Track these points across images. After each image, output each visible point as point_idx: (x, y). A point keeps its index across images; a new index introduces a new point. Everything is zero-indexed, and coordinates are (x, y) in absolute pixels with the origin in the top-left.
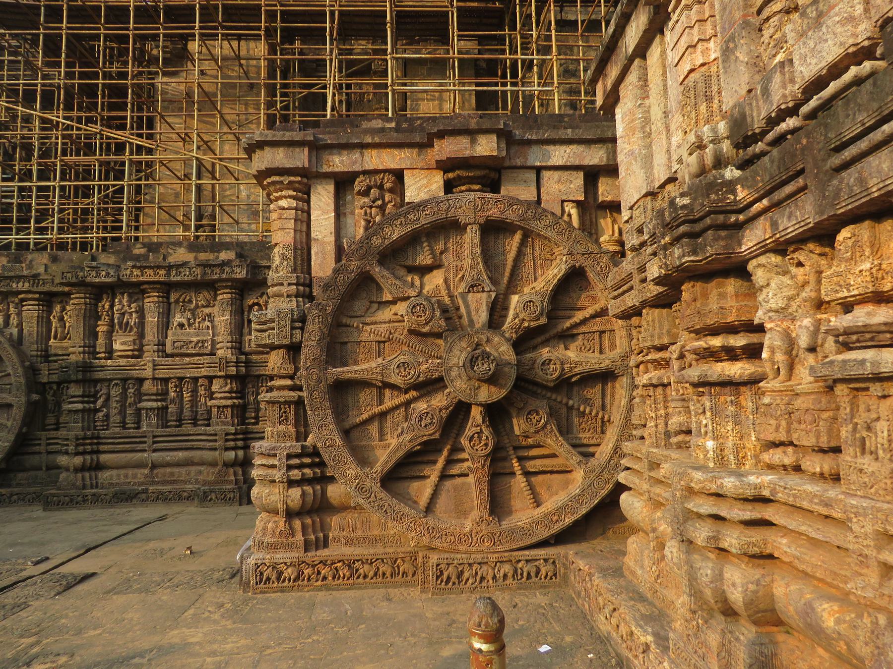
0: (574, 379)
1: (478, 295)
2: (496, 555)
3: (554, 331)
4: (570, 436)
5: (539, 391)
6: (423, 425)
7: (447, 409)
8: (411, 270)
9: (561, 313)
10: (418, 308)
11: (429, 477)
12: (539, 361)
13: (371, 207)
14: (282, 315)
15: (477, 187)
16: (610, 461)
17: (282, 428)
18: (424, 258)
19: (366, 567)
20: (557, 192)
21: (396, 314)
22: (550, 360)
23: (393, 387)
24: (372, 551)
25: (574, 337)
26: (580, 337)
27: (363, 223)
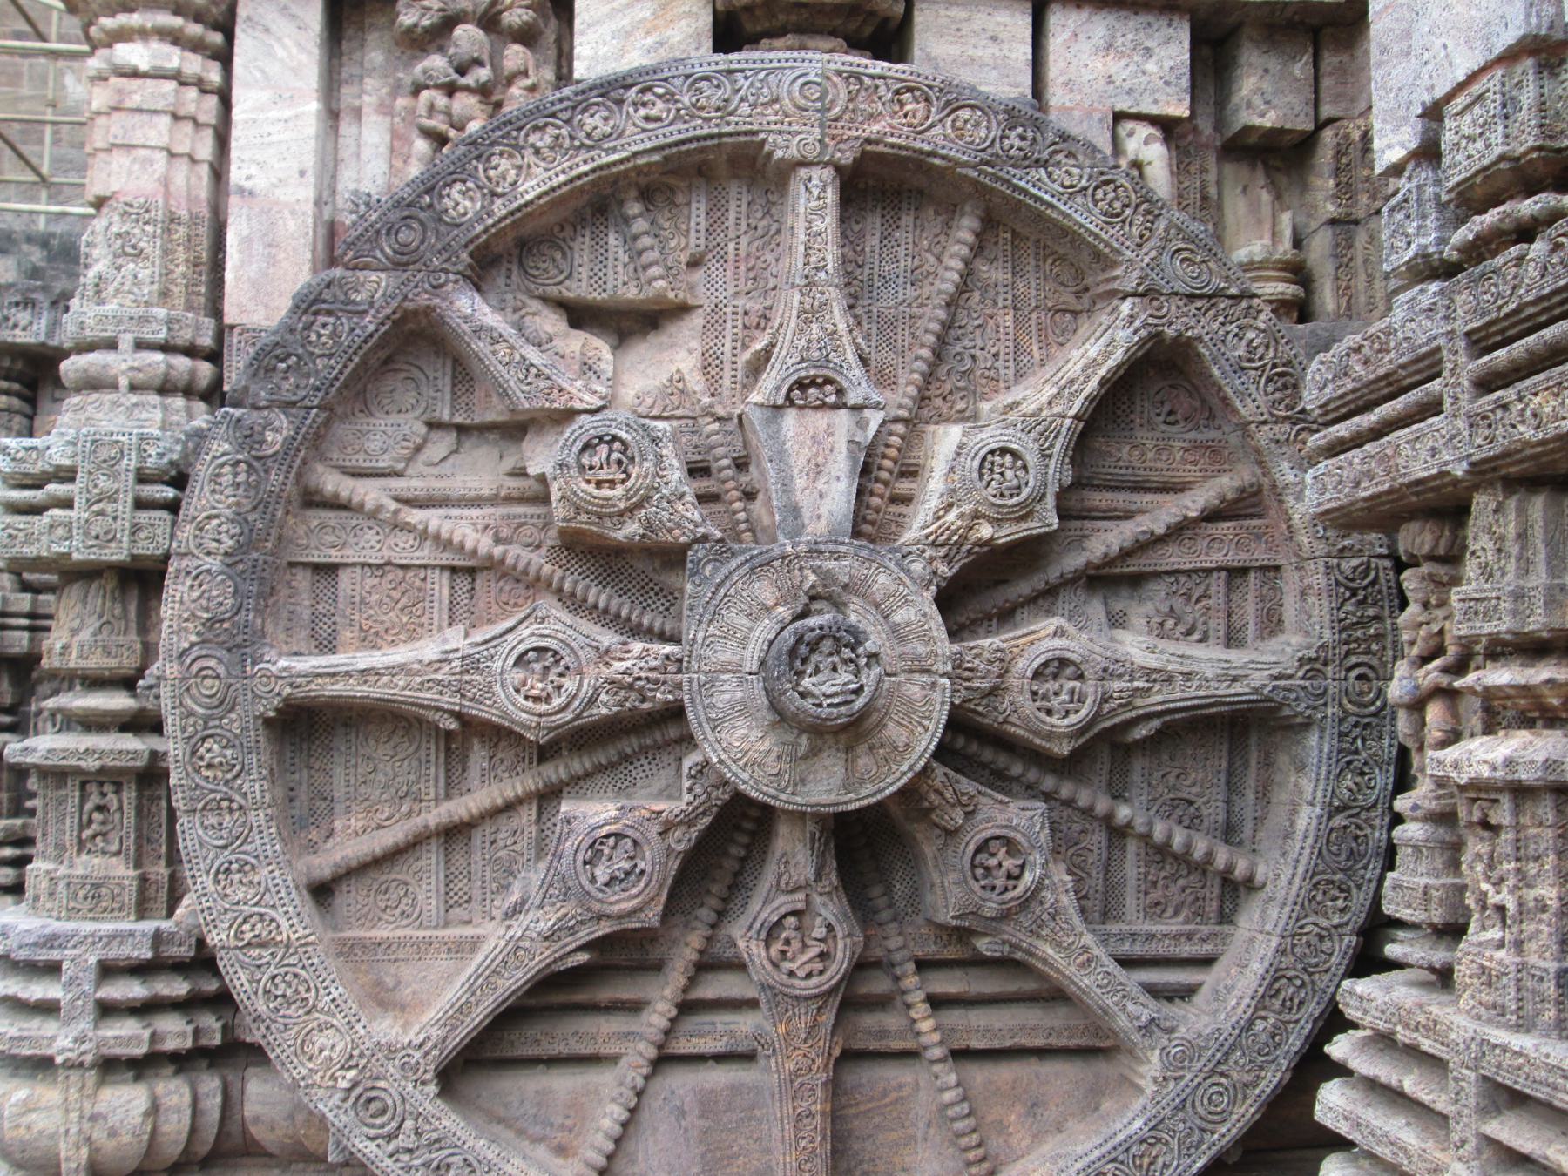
0: (1141, 732)
1: (821, 420)
3: (1073, 561)
4: (1114, 928)
5: (1017, 769)
7: (690, 823)
8: (580, 315)
9: (1100, 499)
10: (603, 450)
11: (614, 1059)
12: (1025, 665)
13: (451, 90)
14: (104, 453)
16: (1251, 1022)
17: (87, 865)
20: (1102, 82)
22: (1063, 662)
23: (498, 735)
25: (1136, 581)
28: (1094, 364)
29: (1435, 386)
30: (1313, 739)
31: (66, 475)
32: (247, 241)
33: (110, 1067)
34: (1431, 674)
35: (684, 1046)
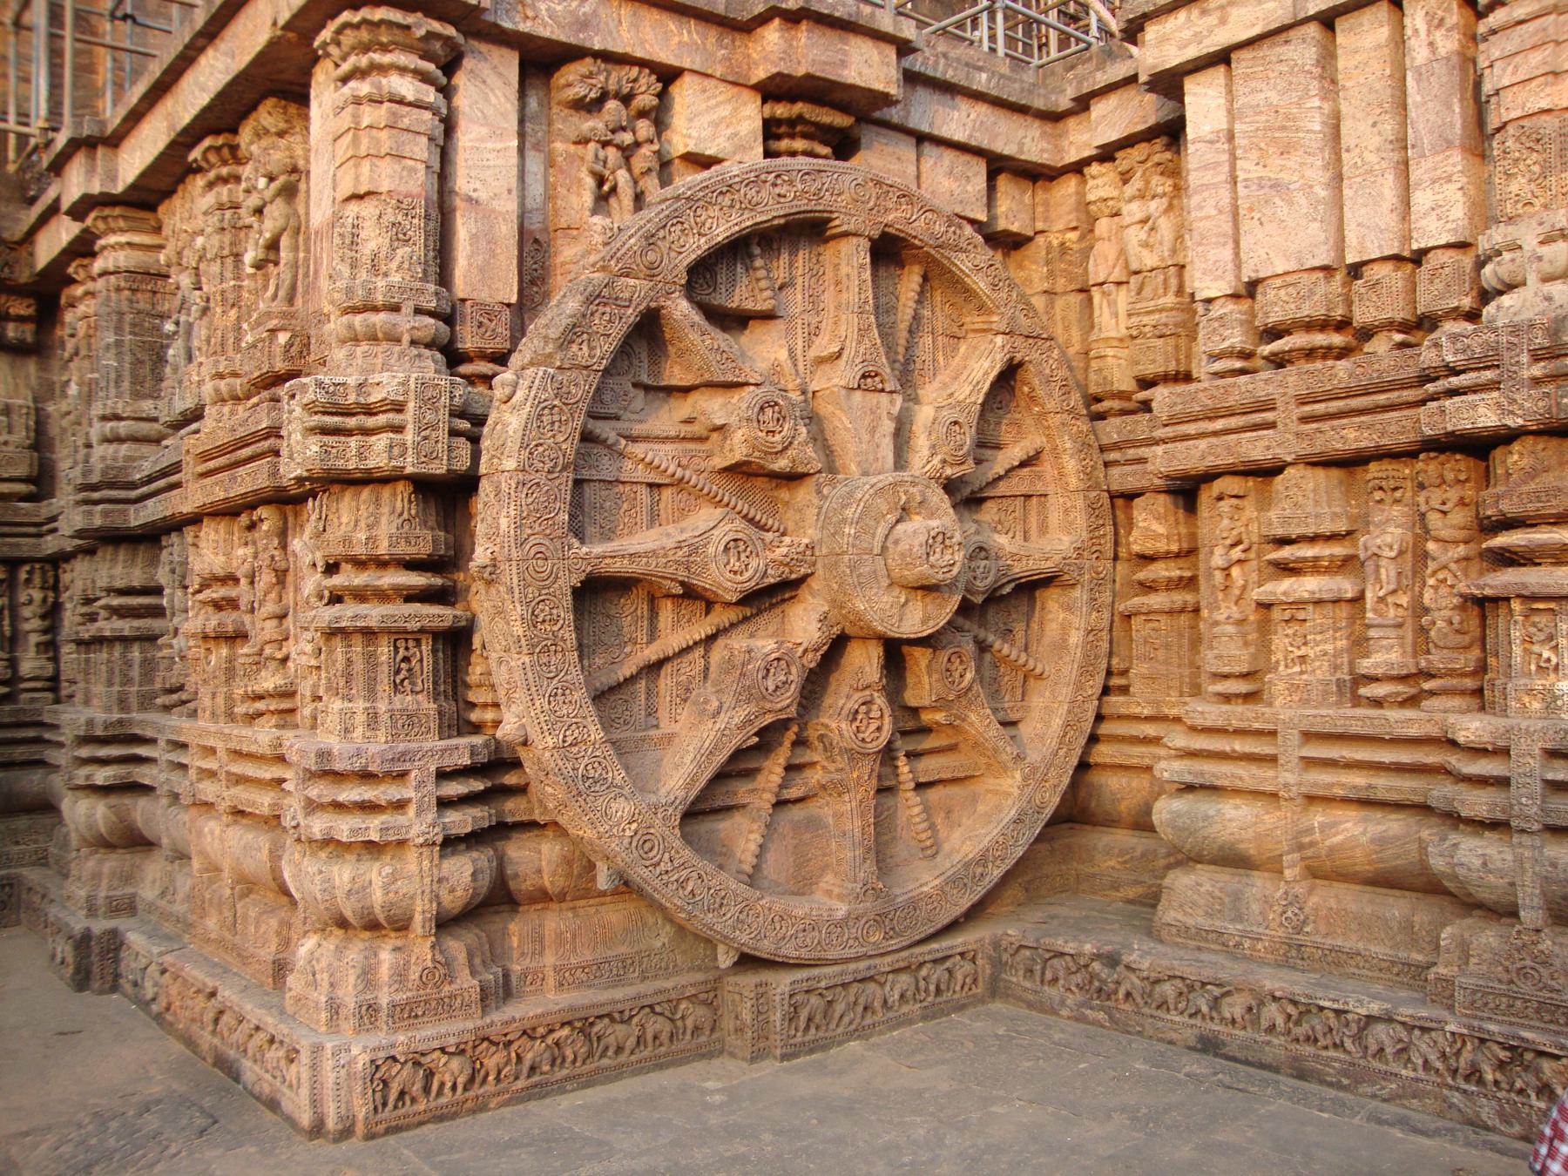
0: (1007, 589)
1: (874, 398)
2: (888, 959)
6: (771, 688)
10: (769, 412)
13: (605, 144)
15: (826, 150)
17: (406, 701)
18: (742, 293)
19: (621, 1029)
20: (947, 195)
21: (689, 421)
22: (981, 549)
24: (630, 991)
25: (982, 500)
26: (989, 504)
27: (590, 182)
28: (986, 373)
29: (1269, 416)
30: (1077, 593)
31: (399, 408)
32: (474, 238)
33: (450, 844)
34: (1236, 553)
35: (793, 793)
